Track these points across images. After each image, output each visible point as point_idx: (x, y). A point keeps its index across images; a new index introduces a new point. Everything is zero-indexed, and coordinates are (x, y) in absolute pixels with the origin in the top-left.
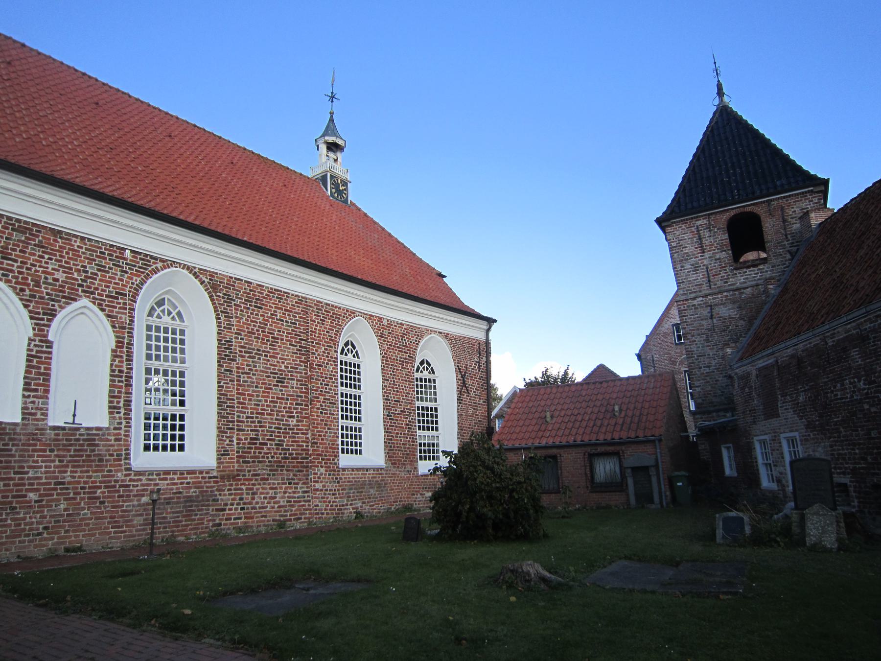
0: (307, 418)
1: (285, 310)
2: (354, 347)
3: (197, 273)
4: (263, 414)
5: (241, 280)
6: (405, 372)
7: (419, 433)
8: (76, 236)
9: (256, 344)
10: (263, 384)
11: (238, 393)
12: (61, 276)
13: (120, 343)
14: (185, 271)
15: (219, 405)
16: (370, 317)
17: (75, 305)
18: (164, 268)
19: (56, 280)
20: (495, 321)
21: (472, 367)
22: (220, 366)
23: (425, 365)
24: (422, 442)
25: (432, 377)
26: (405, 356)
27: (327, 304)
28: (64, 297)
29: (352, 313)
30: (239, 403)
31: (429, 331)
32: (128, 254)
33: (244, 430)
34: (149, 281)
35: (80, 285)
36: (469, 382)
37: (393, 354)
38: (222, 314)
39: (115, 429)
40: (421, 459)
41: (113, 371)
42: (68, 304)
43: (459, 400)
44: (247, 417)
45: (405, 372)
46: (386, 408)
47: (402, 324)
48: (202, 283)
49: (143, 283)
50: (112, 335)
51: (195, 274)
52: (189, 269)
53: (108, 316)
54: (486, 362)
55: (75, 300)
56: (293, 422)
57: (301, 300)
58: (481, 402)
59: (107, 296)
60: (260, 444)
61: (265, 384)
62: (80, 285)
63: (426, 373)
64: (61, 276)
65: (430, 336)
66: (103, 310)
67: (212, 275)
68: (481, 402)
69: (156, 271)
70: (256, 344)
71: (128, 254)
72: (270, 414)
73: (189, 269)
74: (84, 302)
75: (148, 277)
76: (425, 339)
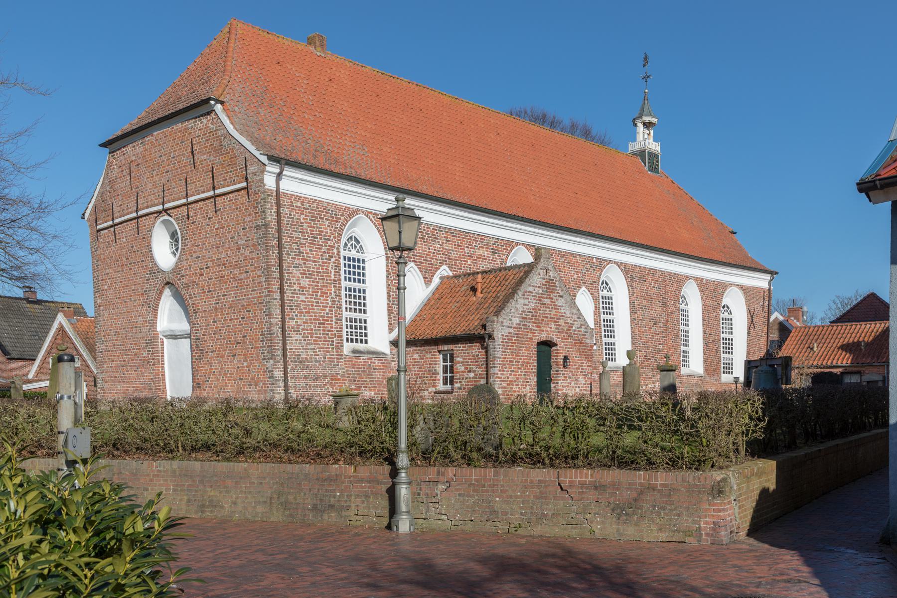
0: (667, 345)
1: (656, 281)
2: (685, 299)
3: (620, 265)
4: (648, 342)
5: (636, 266)
6: (715, 314)
7: (723, 356)
8: (578, 255)
9: (644, 303)
10: (648, 325)
11: (639, 331)
12: (575, 276)
13: (596, 307)
14: (615, 265)
15: (632, 337)
16: (697, 279)
17: (581, 290)
18: (607, 264)
19: (574, 279)
20: (777, 273)
21: (758, 307)
22: (631, 316)
23: (726, 308)
24: (725, 362)
25: (730, 316)
26: (715, 303)
27: (675, 274)
28: (578, 287)
29: (687, 278)
30: (639, 336)
31: (731, 284)
32: (595, 260)
33: (641, 351)
34: (603, 273)
35: (582, 280)
36: (755, 320)
37: (709, 303)
38: (631, 287)
39: (599, 350)
40: (724, 373)
41: (595, 322)
42: (579, 290)
43: (749, 333)
44: (643, 344)
45: (715, 314)
46: (705, 339)
47: (714, 281)
48: (622, 270)
49: (600, 275)
50: (593, 304)
51: (619, 266)
52: (616, 263)
53: (591, 294)
54: (768, 305)
55: (580, 288)
56: (661, 347)
57: (663, 273)
58: (763, 335)
59: (590, 284)
60: (649, 359)
61: (648, 325)
62: (582, 280)
63: (726, 314)
64: (575, 276)
65: (731, 288)
66: (589, 291)
67: (625, 265)
68: (763, 335)
69: (604, 267)
70: (644, 303)
71: (594, 259)
72: (651, 343)
73: (616, 263)
74: (584, 288)
75: (602, 271)
76: (728, 290)
